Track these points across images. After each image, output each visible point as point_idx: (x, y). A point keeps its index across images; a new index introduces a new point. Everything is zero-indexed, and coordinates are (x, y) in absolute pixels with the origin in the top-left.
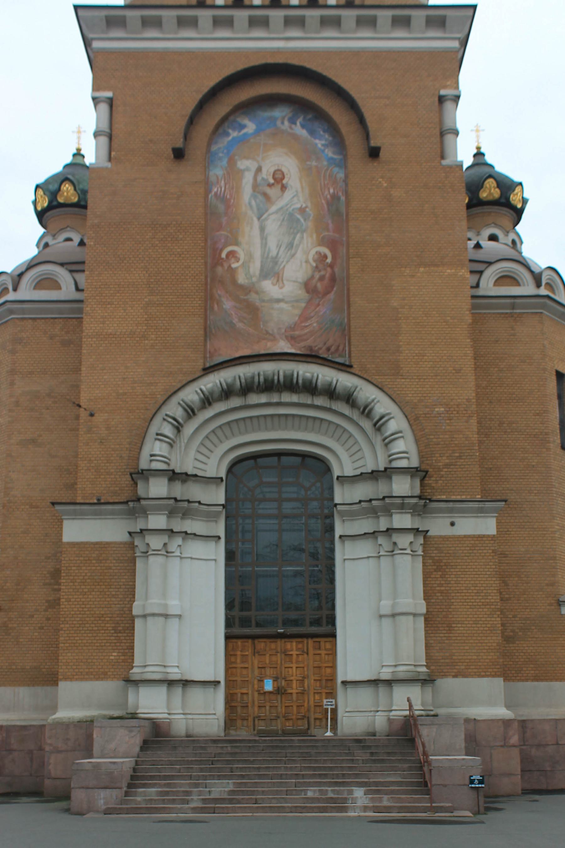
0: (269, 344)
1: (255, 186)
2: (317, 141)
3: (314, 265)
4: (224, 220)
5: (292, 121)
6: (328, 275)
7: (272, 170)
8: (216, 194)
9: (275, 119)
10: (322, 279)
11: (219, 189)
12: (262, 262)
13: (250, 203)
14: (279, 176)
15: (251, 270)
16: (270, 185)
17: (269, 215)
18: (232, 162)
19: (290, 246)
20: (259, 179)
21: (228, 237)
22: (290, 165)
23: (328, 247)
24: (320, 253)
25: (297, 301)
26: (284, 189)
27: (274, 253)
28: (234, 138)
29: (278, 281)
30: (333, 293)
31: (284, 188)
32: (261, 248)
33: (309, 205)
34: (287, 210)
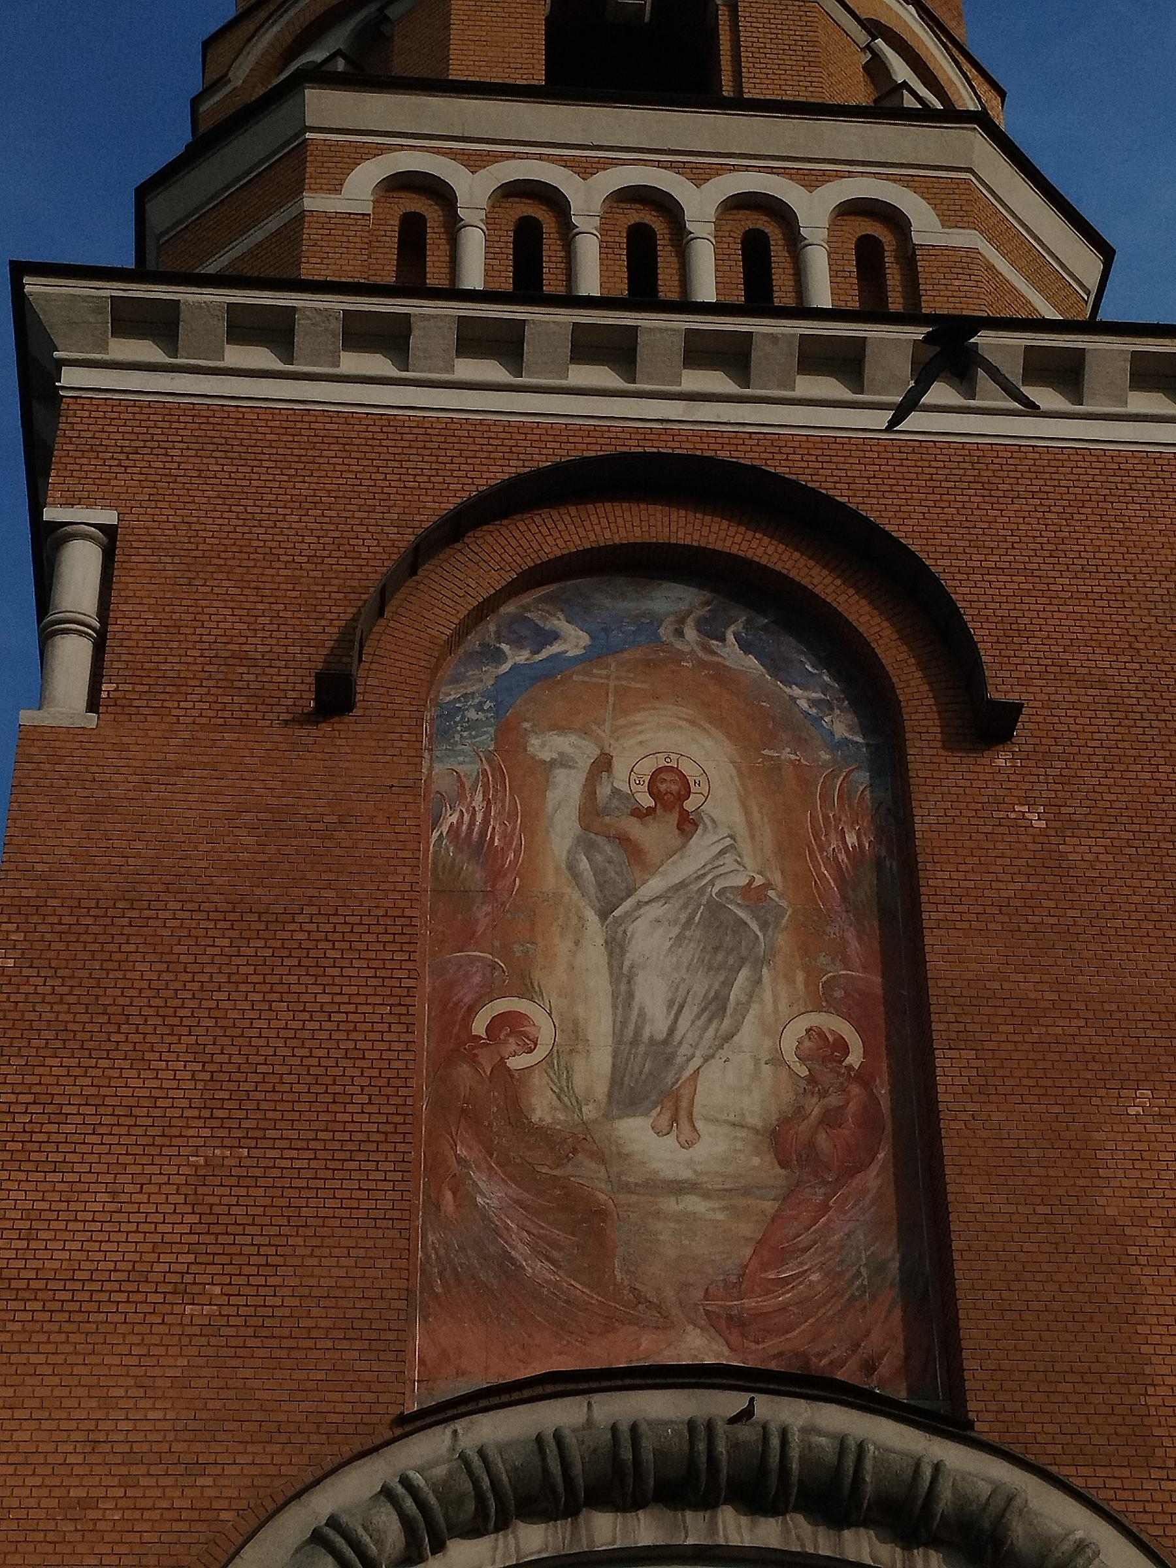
0: (647, 1341)
1: (591, 813)
2: (796, 691)
3: (804, 1072)
4: (482, 913)
5: (711, 629)
6: (852, 1107)
7: (647, 767)
8: (454, 830)
9: (656, 621)
10: (831, 1119)
11: (466, 817)
12: (615, 1055)
13: (572, 867)
15: (579, 1081)
16: (640, 813)
17: (639, 905)
18: (509, 739)
19: (716, 1005)
20: (603, 791)
21: (493, 966)
22: (708, 758)
23: (848, 1018)
24: (822, 1035)
25: (746, 1192)
26: (688, 827)
27: (658, 1025)
28: (515, 667)
29: (674, 1119)
30: (874, 1170)
31: (688, 824)
32: (615, 1007)
33: (777, 878)
34: (701, 891)
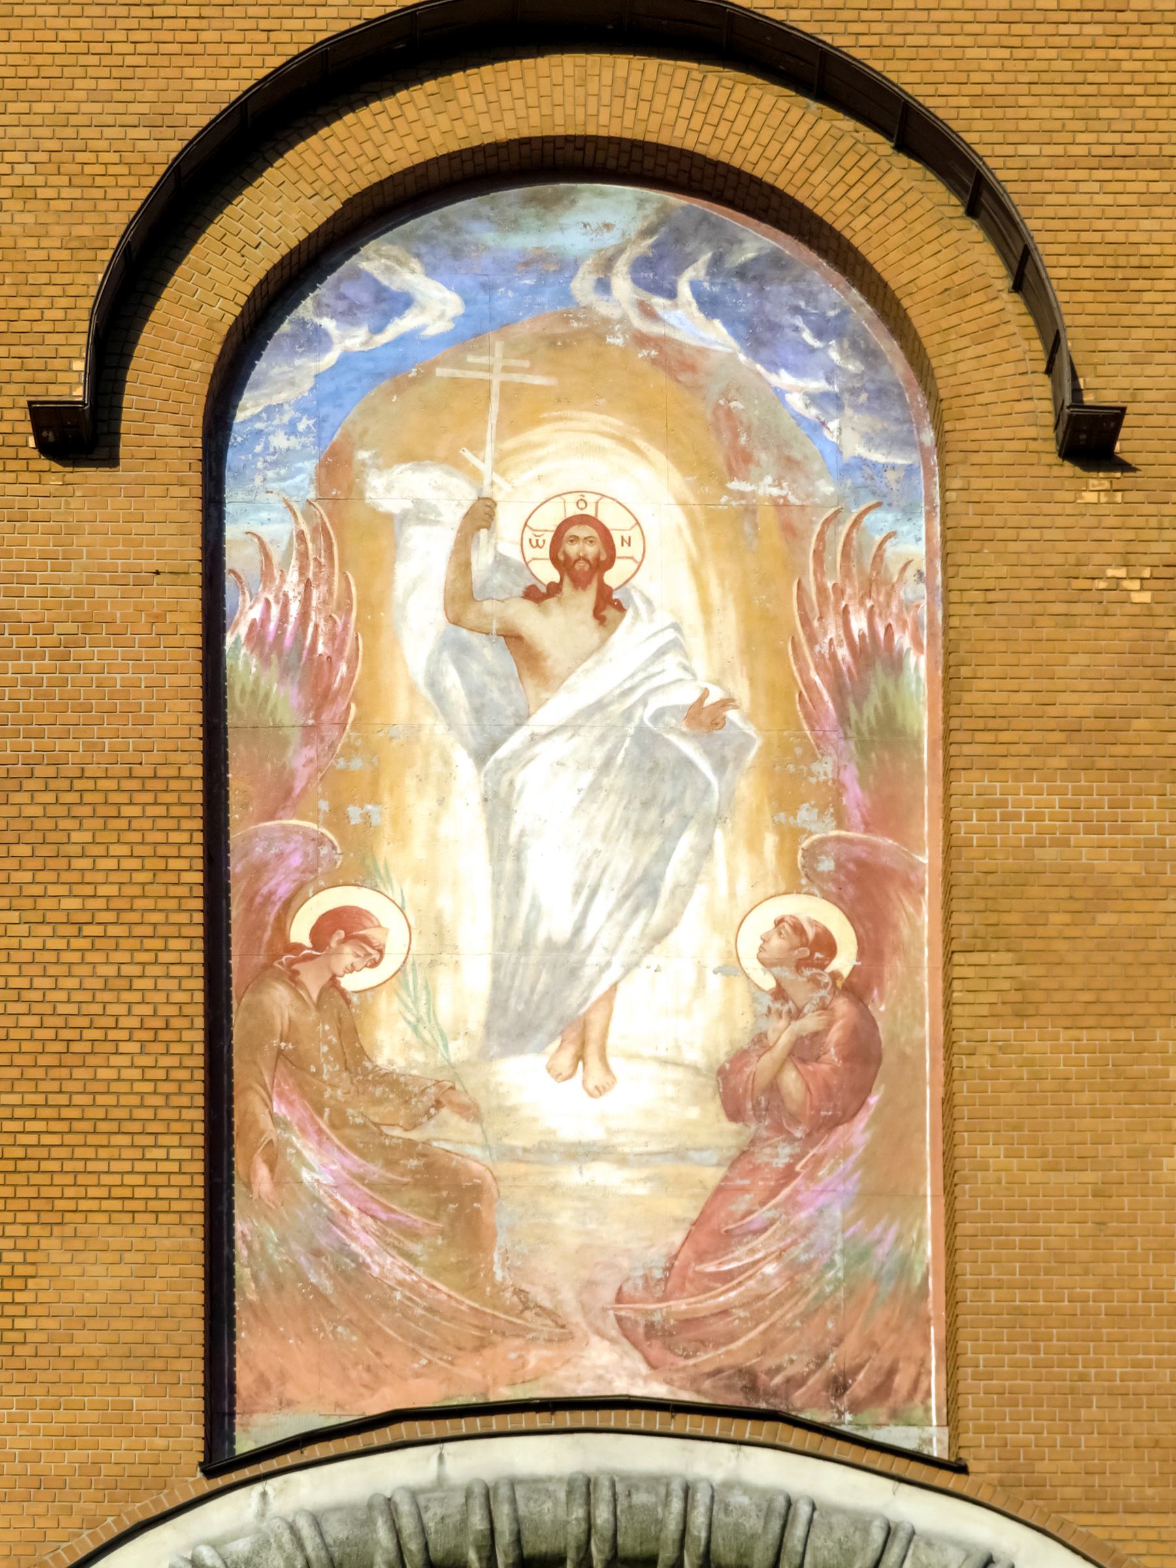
1: (461, 599)
10: (804, 1051)
14: (583, 548)
16: (534, 595)
20: (482, 560)
22: (644, 496)
31: (608, 608)
